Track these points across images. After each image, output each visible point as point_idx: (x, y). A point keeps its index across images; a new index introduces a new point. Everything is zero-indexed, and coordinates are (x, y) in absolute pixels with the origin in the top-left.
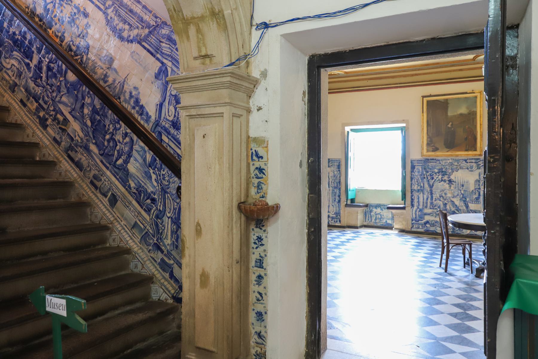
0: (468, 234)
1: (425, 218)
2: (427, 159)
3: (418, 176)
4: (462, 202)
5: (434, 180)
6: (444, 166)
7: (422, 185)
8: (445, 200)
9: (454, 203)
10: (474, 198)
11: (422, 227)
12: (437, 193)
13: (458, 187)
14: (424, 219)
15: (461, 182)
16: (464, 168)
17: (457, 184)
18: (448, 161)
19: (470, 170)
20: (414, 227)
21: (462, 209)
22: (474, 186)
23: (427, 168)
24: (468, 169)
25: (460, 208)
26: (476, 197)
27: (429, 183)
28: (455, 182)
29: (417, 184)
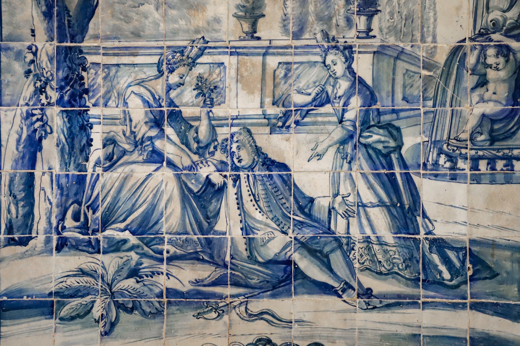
9: (287, 181)
10: (472, 122)
21: (355, 233)
26: (490, 108)
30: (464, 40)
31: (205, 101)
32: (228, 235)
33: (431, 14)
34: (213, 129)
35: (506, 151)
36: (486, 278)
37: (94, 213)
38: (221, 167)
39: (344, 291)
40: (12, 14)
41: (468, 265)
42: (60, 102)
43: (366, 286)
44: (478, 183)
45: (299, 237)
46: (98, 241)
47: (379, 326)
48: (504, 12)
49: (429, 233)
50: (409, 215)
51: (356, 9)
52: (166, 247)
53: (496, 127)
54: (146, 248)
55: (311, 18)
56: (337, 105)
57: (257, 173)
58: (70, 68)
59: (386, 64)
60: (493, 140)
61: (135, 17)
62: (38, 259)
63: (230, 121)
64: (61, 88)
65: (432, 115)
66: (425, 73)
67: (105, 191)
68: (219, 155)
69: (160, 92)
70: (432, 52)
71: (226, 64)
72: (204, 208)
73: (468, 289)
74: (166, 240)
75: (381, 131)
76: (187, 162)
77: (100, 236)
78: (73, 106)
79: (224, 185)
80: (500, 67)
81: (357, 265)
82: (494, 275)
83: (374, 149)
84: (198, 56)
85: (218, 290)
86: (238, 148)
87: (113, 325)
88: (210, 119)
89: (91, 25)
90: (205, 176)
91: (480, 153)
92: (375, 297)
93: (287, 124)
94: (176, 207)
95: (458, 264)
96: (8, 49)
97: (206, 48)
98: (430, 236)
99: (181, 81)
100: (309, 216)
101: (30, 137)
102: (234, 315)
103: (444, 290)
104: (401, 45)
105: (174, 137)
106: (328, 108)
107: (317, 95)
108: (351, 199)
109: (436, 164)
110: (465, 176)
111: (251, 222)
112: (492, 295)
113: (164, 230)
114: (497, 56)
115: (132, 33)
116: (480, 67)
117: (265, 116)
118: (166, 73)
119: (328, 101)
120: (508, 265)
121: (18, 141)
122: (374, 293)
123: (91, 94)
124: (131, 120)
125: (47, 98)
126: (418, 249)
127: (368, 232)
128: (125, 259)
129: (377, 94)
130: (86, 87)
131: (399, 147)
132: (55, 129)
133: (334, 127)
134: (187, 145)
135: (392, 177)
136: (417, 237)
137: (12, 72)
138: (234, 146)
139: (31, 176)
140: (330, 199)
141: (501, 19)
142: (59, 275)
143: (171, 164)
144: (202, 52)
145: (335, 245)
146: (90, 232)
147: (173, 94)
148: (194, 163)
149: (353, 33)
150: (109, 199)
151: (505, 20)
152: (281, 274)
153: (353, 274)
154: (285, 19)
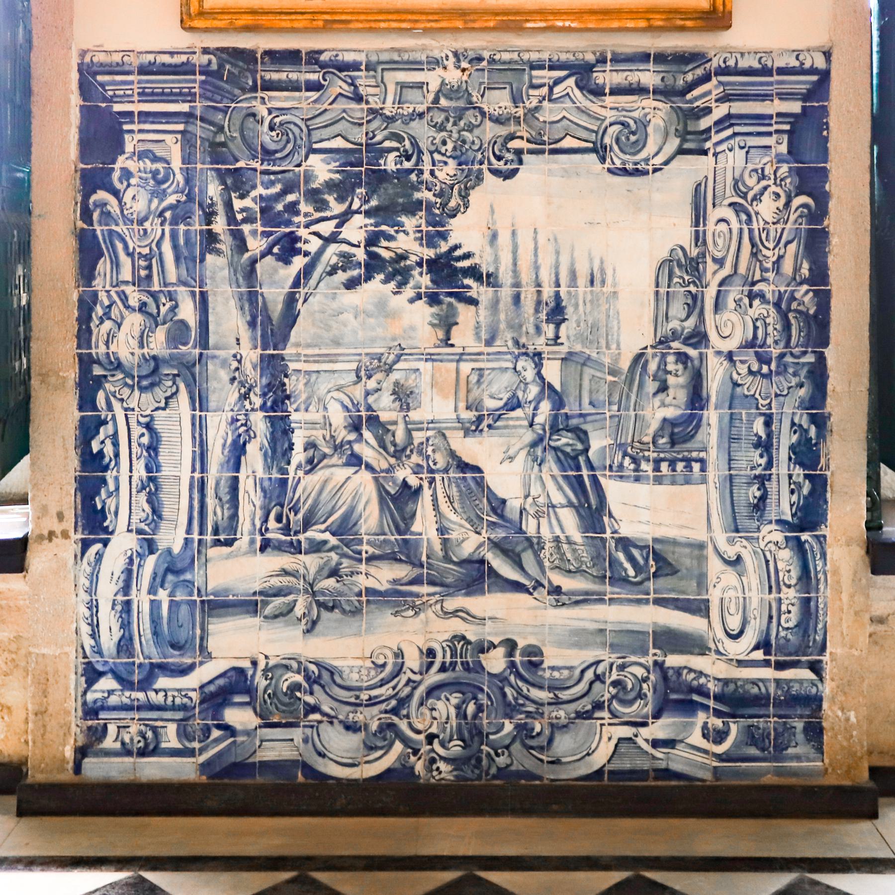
0: (599, 773)
1: (212, 644)
2: (237, 54)
3: (154, 227)
4: (551, 466)
5: (299, 262)
6: (397, 127)
7: (188, 312)
8: (399, 453)
9: (480, 483)
10: (654, 425)
11: (183, 733)
12: (323, 386)
13: (516, 326)
14: (206, 654)
15: (546, 276)
16: (568, 143)
17: (506, 293)
18: (433, 78)
19: (618, 159)
20: (109, 743)
21: (546, 533)
22: (648, 313)
23: (237, 147)
24: (600, 151)
25: (530, 527)
26: (671, 413)
27: (252, 297)
28: (491, 280)
30: (646, 348)
31: (401, 405)
32: (424, 536)
33: (615, 323)
34: (409, 432)
35: (686, 454)
36: (667, 575)
37: (295, 515)
38: (417, 470)
39: (535, 588)
40: (218, 324)
41: (652, 562)
42: (263, 408)
43: (555, 584)
44: (660, 484)
45: (492, 536)
46: (299, 542)
47: (568, 622)
48: (682, 321)
49: (615, 532)
50: (596, 515)
51: (545, 318)
52: (365, 547)
53: (676, 430)
54: (345, 549)
55: (502, 326)
56: (527, 409)
57: (452, 475)
58: (272, 375)
59: (573, 368)
60: (673, 443)
61: (335, 325)
62: (244, 560)
63: (425, 425)
64: (264, 395)
65: (617, 419)
66: (610, 378)
67: (306, 494)
68: (415, 459)
69: (358, 397)
70: (617, 358)
71: (421, 370)
72: (400, 510)
73: (651, 585)
74: (365, 541)
75: (569, 434)
76: (385, 466)
77: (301, 537)
78: (275, 411)
79: (420, 488)
80: (679, 373)
81: (547, 564)
82: (675, 572)
83: (563, 452)
84: (395, 362)
85: (415, 589)
86: (434, 451)
87: (314, 623)
88: (406, 423)
89: (293, 333)
90: (401, 479)
91: (662, 455)
92: (565, 594)
93: (480, 428)
94: (374, 508)
95: (641, 562)
96: (214, 357)
97: (402, 355)
98: (616, 536)
99: (379, 387)
100: (501, 516)
101: (235, 442)
102: (430, 612)
103: (629, 587)
104: (588, 352)
105: (373, 441)
106: (518, 413)
107: (509, 399)
108: (541, 500)
109: (621, 466)
110: (648, 477)
111: (447, 524)
112: (672, 590)
113: (363, 531)
114: (676, 362)
115: (332, 341)
116: (660, 373)
117: (459, 420)
118: (364, 379)
119: (519, 405)
120: (687, 562)
121: (224, 445)
122: (564, 590)
123: (292, 400)
124: (330, 425)
125: (251, 403)
126: (605, 547)
127: (558, 532)
128: (326, 559)
129: (565, 399)
130: (288, 392)
131: (587, 450)
132: (258, 434)
133: (525, 431)
134: (385, 448)
135: (580, 478)
136: (604, 536)
137: (219, 380)
138: (430, 449)
139: (236, 480)
140: (521, 501)
141: (679, 328)
142: (264, 575)
143: (369, 467)
144: (398, 359)
145: (526, 544)
146: (292, 533)
147: (371, 399)
148: (391, 466)
149: (542, 340)
150: (310, 502)
151: (683, 329)
152: (475, 573)
153: (543, 572)
154: (478, 327)
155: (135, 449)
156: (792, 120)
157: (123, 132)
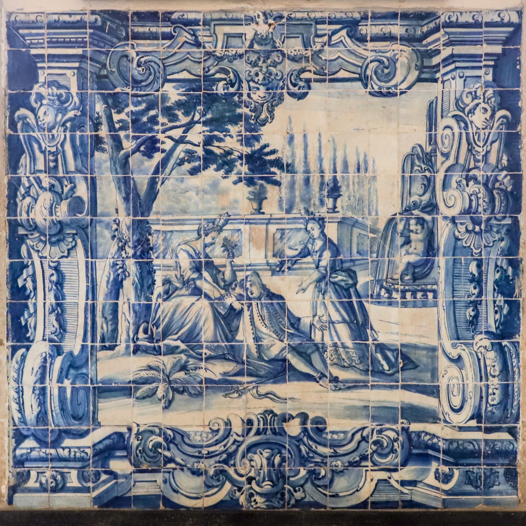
0: (364, 504)
1: (101, 417)
2: (115, 15)
3: (59, 133)
4: (331, 295)
5: (158, 157)
6: (225, 64)
8: (227, 287)
9: (283, 307)
10: (401, 268)
11: (82, 477)
12: (176, 240)
13: (307, 200)
14: (97, 424)
15: (327, 166)
16: (342, 74)
17: (300, 177)
18: (249, 31)
19: (376, 85)
20: (32, 483)
21: (328, 341)
22: (397, 191)
23: (115, 78)
24: (364, 80)
25: (317, 337)
26: (413, 259)
27: (126, 181)
28: (290, 168)
29: (52, 188)
30: (396, 214)
31: (229, 255)
32: (244, 343)
33: (375, 197)
34: (234, 272)
35: (423, 286)
36: (411, 369)
37: (157, 329)
38: (240, 298)
39: (320, 378)
40: (103, 199)
41: (400, 360)
42: (134, 256)
43: (334, 375)
44: (406, 307)
45: (291, 343)
46: (160, 347)
47: (343, 401)
48: (420, 196)
49: (375, 340)
50: (362, 328)
51: (326, 194)
52: (204, 351)
53: (417, 270)
54: (191, 352)
55: (298, 200)
56: (314, 257)
57: (263, 301)
58: (140, 234)
59: (346, 230)
60: (415, 279)
61: (183, 200)
62: (121, 359)
63: (245, 268)
64: (135, 247)
65: (376, 263)
66: (371, 235)
67: (164, 314)
68: (238, 290)
69: (199, 248)
70: (376, 222)
71: (242, 230)
72: (228, 325)
73: (400, 376)
74: (204, 346)
75: (343, 274)
76: (217, 295)
77: (161, 344)
78: (143, 258)
79: (241, 311)
80: (419, 231)
81: (328, 361)
82: (416, 367)
83: (339, 286)
84: (224, 225)
85: (238, 379)
86: (251, 285)
87: (170, 402)
88: (232, 266)
89: (154, 205)
90: (229, 304)
91: (407, 288)
92: (341, 382)
93: (283, 269)
94: (210, 324)
95: (393, 360)
96: (101, 222)
97: (229, 220)
98: (375, 342)
99: (213, 241)
100: (297, 329)
101: (115, 280)
102: (249, 395)
103: (384, 377)
104: (356, 217)
105: (209, 279)
106: (309, 259)
107: (302, 250)
108: (324, 318)
109: (379, 295)
110: (397, 302)
111: (260, 335)
112: (415, 379)
113: (203, 340)
114: (416, 224)
115: (181, 210)
116: (406, 231)
117: (268, 264)
118: (203, 236)
119: (309, 254)
120: (425, 360)
121: (108, 282)
122: (340, 379)
123: (154, 250)
124: (180, 267)
125: (126, 253)
126: (368, 350)
127: (336, 340)
128: (178, 359)
129: (341, 249)
130: (151, 245)
131: (355, 284)
132: (131, 274)
133: (313, 271)
134: (218, 284)
135: (351, 304)
136: (367, 342)
137: (104, 237)
138: (248, 284)
139: (116, 305)
140: (311, 319)
141: (418, 201)
142: (135, 370)
143: (207, 296)
144: (226, 222)
145: (314, 348)
146: (155, 341)
147: (208, 250)
148: (222, 295)
149: (324, 209)
150: (167, 320)
151: (421, 201)
152: (279, 368)
153: (326, 367)
154: (280, 200)
155: (48, 284)
156: (495, 58)
157: (37, 68)
